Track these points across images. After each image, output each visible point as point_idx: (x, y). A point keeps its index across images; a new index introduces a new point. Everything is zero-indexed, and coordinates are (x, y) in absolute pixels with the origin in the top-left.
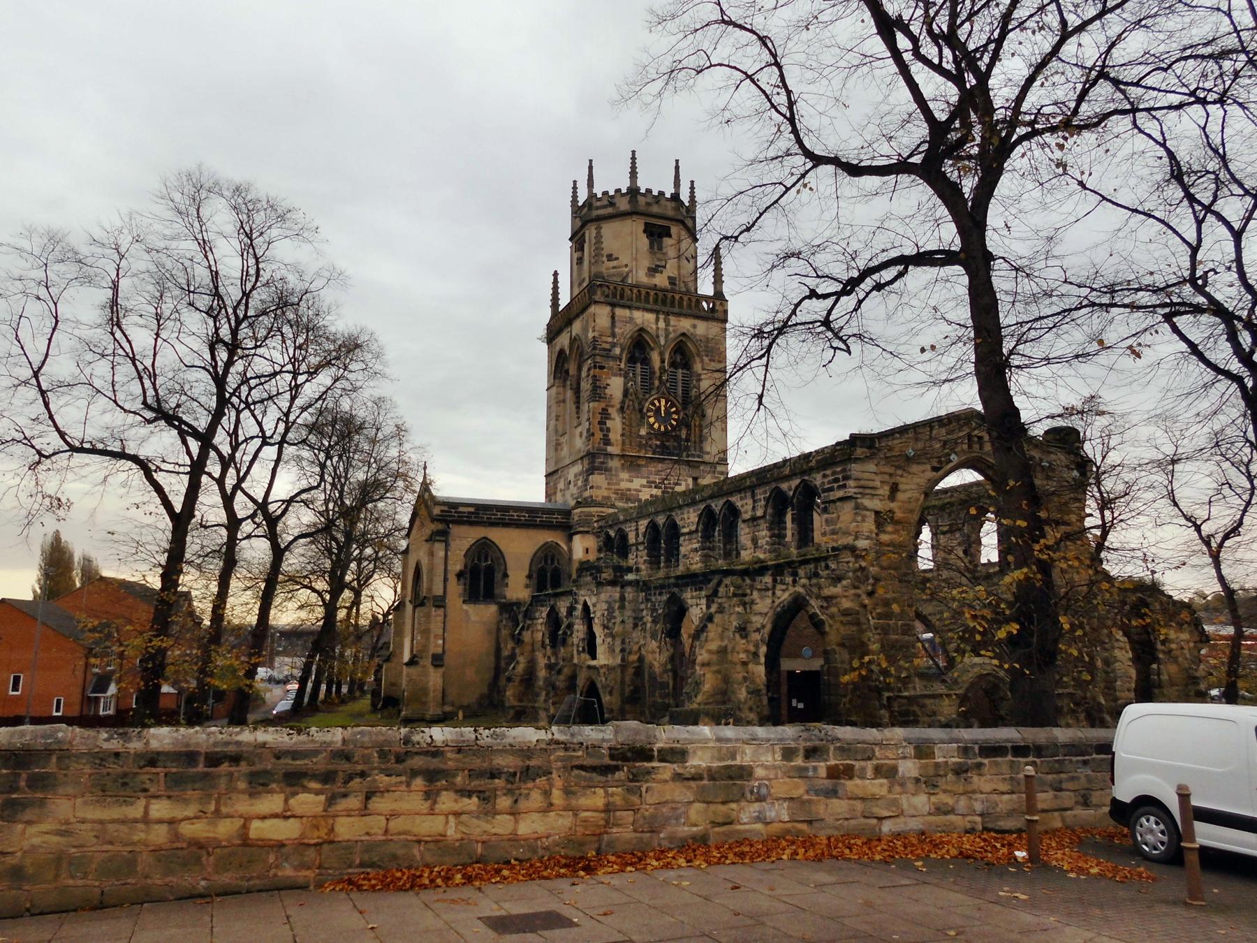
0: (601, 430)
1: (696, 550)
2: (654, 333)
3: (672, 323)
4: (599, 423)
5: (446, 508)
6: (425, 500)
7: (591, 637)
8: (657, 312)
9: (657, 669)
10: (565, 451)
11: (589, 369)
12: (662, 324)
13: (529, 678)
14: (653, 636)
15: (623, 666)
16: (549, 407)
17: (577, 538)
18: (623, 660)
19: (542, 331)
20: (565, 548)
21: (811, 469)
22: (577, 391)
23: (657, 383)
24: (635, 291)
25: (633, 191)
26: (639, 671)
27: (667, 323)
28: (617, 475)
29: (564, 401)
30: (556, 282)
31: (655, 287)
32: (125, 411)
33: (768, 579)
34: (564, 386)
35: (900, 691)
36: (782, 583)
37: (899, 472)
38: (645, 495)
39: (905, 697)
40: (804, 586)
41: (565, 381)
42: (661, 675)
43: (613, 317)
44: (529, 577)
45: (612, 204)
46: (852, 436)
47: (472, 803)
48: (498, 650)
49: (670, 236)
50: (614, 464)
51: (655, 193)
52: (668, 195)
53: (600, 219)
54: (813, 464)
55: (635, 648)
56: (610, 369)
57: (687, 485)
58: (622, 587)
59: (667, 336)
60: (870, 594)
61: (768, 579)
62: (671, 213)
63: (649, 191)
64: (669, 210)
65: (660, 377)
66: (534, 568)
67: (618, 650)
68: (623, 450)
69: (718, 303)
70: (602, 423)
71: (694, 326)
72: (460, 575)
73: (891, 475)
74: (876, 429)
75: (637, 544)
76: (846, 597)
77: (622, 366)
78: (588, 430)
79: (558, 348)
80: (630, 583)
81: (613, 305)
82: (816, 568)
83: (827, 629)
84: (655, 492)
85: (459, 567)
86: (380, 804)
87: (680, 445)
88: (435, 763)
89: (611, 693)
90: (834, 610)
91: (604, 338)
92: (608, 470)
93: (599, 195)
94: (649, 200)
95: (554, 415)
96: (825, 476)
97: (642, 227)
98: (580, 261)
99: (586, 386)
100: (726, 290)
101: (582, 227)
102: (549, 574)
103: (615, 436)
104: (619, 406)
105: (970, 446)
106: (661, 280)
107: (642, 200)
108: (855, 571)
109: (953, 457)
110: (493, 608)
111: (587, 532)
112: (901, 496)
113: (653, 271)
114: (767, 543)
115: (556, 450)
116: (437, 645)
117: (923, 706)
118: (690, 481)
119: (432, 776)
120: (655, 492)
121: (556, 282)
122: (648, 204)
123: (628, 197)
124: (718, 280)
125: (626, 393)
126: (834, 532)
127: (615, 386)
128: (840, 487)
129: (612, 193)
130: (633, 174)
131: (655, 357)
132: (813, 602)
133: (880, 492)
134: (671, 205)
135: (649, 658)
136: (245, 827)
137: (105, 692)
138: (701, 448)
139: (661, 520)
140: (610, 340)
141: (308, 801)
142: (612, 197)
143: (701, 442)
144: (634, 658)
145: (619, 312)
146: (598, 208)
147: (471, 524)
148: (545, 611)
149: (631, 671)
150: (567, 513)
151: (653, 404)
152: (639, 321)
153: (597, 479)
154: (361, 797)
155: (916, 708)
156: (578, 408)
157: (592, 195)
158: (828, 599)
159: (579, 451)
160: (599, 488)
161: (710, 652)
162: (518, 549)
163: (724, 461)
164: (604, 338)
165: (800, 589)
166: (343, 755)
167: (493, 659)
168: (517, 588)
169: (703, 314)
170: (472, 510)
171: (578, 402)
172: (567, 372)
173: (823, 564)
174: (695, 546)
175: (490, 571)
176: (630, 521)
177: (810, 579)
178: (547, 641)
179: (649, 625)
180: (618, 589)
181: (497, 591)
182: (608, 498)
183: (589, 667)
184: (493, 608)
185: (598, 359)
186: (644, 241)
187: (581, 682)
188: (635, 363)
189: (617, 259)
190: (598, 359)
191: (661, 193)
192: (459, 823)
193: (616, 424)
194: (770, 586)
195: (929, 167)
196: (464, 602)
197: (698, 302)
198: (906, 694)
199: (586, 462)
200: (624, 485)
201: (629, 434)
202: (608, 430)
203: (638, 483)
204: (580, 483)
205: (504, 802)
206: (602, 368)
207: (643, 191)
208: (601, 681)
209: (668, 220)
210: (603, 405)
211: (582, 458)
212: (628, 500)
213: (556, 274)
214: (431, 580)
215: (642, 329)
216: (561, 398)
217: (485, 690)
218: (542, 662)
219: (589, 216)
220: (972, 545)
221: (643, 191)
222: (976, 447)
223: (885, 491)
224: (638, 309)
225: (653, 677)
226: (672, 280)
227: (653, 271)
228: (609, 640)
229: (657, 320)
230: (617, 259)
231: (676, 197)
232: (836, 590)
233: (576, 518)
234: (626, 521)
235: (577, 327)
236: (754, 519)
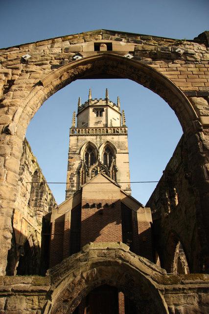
12: (98, 139)
27: (101, 139)
71: (113, 138)
73: (6, 74)
94: (96, 101)
113: (97, 123)
140: (76, 148)
229: (96, 139)
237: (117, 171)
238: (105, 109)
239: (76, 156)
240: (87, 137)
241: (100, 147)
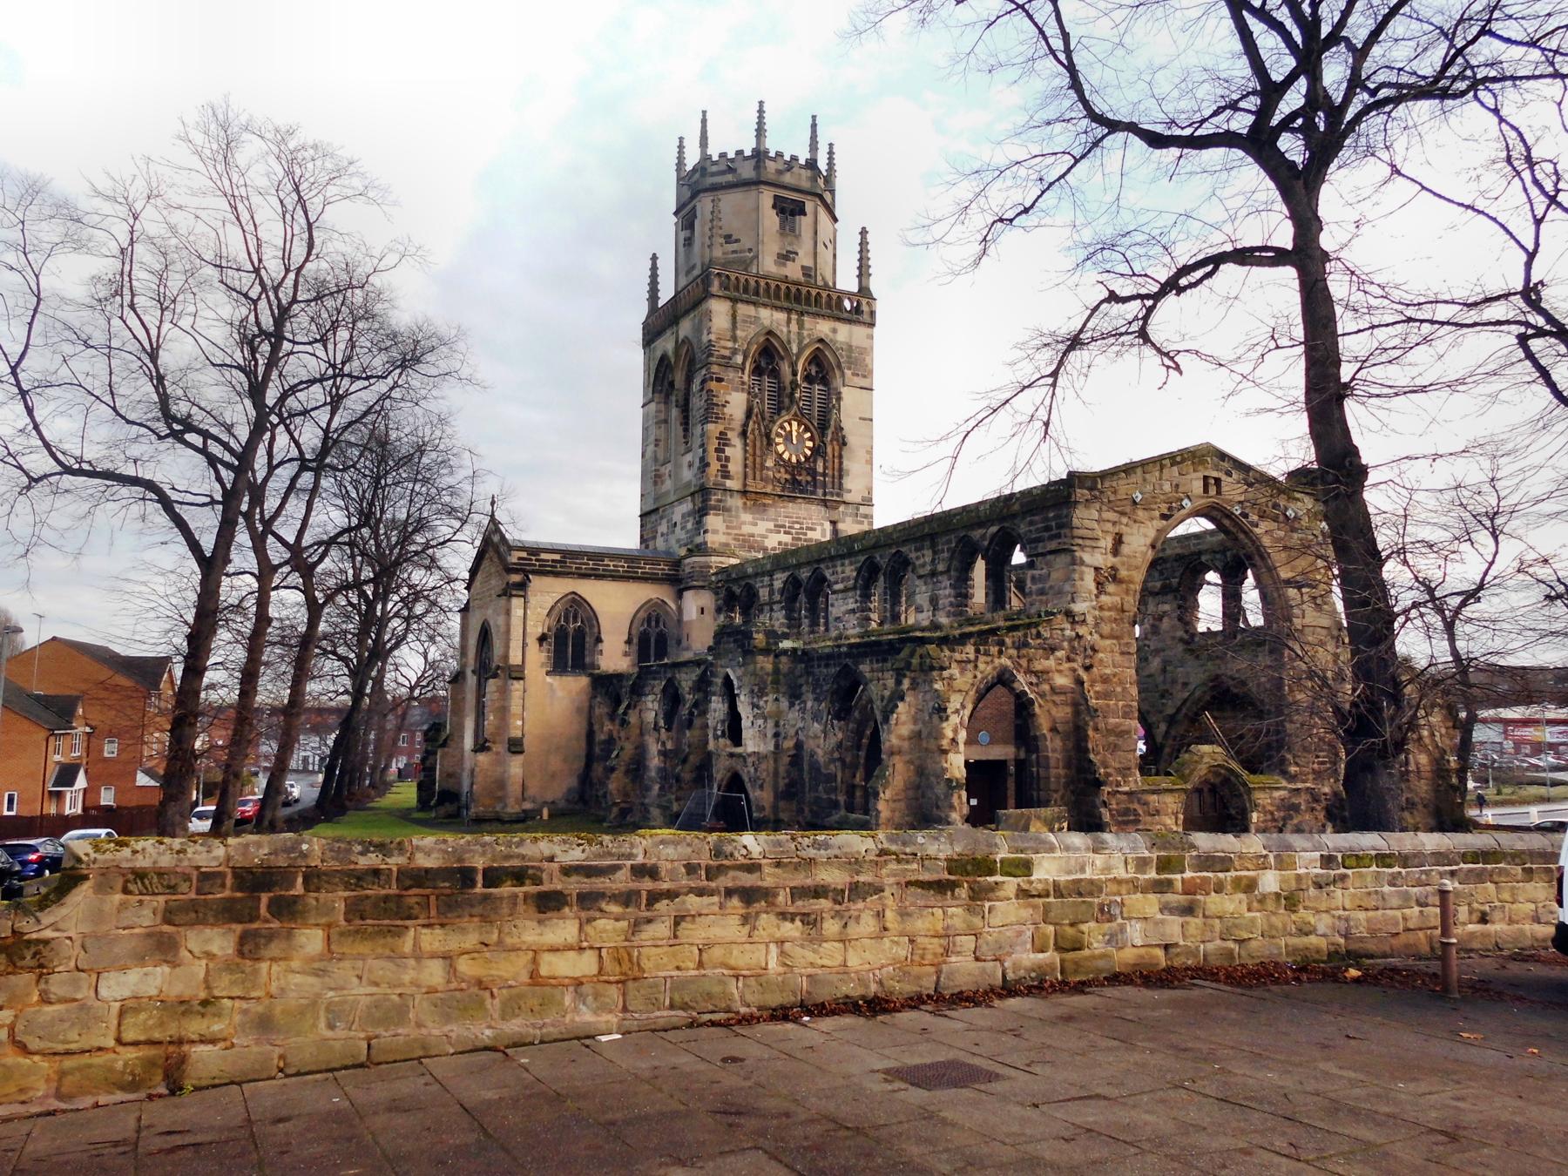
0: (719, 459)
1: (853, 611)
2: (784, 339)
3: (807, 325)
4: (717, 450)
5: (524, 555)
6: (493, 546)
7: (734, 720)
8: (789, 311)
9: (821, 755)
10: (668, 485)
11: (703, 382)
12: (794, 327)
13: (637, 767)
14: (816, 717)
16: (645, 429)
17: (688, 595)
18: (777, 746)
19: (638, 335)
20: (673, 606)
21: (1014, 516)
22: (685, 409)
23: (787, 400)
24: (762, 283)
25: (759, 155)
26: (796, 759)
27: (801, 325)
28: (737, 517)
29: (666, 421)
30: (654, 268)
31: (785, 280)
32: (128, 422)
33: (970, 649)
34: (666, 403)
35: (1119, 785)
36: (987, 654)
37: (1125, 520)
39: (1126, 793)
40: (1010, 658)
41: (667, 396)
42: (827, 767)
43: (734, 317)
44: (629, 642)
45: (731, 170)
46: (1071, 474)
47: (792, 929)
48: (590, 735)
50: (736, 502)
51: (787, 158)
52: (802, 161)
53: (715, 188)
54: (1016, 507)
55: (792, 732)
56: (730, 381)
57: (824, 531)
58: (776, 656)
59: (800, 342)
60: (1088, 668)
61: (970, 649)
62: (806, 185)
63: (779, 155)
64: (802, 179)
65: (792, 394)
66: (634, 632)
67: (770, 734)
68: (745, 485)
69: (864, 301)
71: (834, 331)
72: (542, 639)
73: (1114, 523)
74: (1098, 467)
75: (771, 603)
76: (1060, 671)
77: (746, 378)
78: (702, 459)
79: (659, 354)
80: (785, 652)
81: (734, 301)
82: (1025, 636)
83: (1037, 710)
84: (787, 539)
85: (539, 631)
86: (695, 933)
87: (814, 479)
88: (748, 880)
89: (761, 787)
90: (1046, 687)
91: (723, 343)
92: (727, 510)
93: (715, 158)
94: (781, 167)
95: (652, 438)
96: (1031, 523)
97: (771, 202)
98: (689, 242)
99: (697, 403)
100: (875, 286)
101: (693, 197)
102: (653, 637)
103: (735, 467)
104: (739, 429)
105: (1206, 490)
106: (793, 271)
107: (771, 166)
108: (1071, 640)
109: (1186, 502)
110: (583, 682)
111: (702, 587)
112: (1125, 549)
113: (786, 257)
114: (951, 604)
115: (655, 483)
116: (516, 728)
117: (1146, 804)
118: (828, 526)
119: (749, 896)
121: (654, 268)
122: (779, 172)
123: (753, 162)
124: (863, 270)
125: (749, 413)
126: (1042, 592)
127: (736, 403)
128: (1051, 538)
129: (731, 155)
130: (760, 131)
132: (1020, 677)
133: (1102, 543)
134: (806, 173)
135: (810, 744)
136: (535, 961)
137: (71, 784)
138: (841, 484)
139: (805, 574)
140: (730, 344)
141: (609, 927)
142: (732, 160)
143: (841, 477)
144: (788, 744)
145: (743, 309)
146: (713, 174)
147: (557, 574)
148: (659, 685)
149: (786, 760)
150: (677, 563)
151: (782, 427)
153: (713, 521)
154: (669, 922)
155: (1136, 806)
156: (686, 430)
157: (705, 158)
158: (1042, 675)
159: (688, 484)
160: (715, 532)
161: (901, 738)
162: (616, 606)
163: (868, 502)
164: (723, 343)
165: (1005, 661)
167: (583, 744)
168: (614, 656)
169: (846, 315)
170: (557, 557)
171: (685, 423)
172: (672, 384)
173: (1034, 631)
174: (851, 606)
175: (580, 635)
176: (763, 574)
177: (1018, 649)
178: (662, 723)
179: (809, 704)
180: (771, 658)
181: (587, 660)
182: (727, 545)
183: (732, 755)
184: (583, 682)
185: (715, 369)
186: (771, 219)
187: (720, 771)
188: (760, 375)
189: (737, 241)
190: (715, 369)
191: (794, 158)
192: (782, 953)
193: (735, 452)
194: (972, 657)
195: (1259, 143)
196: (548, 673)
197: (840, 301)
198: (1126, 789)
199: (698, 499)
200: (747, 529)
201: (753, 465)
202: (727, 459)
204: (689, 526)
205: (831, 927)
206: (720, 380)
207: (772, 154)
208: (747, 773)
209: (801, 192)
210: (721, 428)
211: (692, 494)
212: (751, 548)
213: (654, 258)
214: (507, 647)
215: (770, 333)
216: (662, 416)
217: (573, 782)
218: (653, 748)
219: (703, 185)
220: (1188, 607)
221: (772, 154)
222: (1213, 491)
223: (1108, 542)
224: (765, 305)
225: (815, 767)
226: (806, 271)
227: (786, 257)
228: (760, 722)
229: (789, 321)
230: (737, 241)
231: (812, 164)
232: (1050, 663)
233: (688, 570)
234: (756, 575)
235: (685, 328)
236: (933, 574)
237: (845, 444)
238: (809, 207)
239: (731, 375)
241: (798, 355)
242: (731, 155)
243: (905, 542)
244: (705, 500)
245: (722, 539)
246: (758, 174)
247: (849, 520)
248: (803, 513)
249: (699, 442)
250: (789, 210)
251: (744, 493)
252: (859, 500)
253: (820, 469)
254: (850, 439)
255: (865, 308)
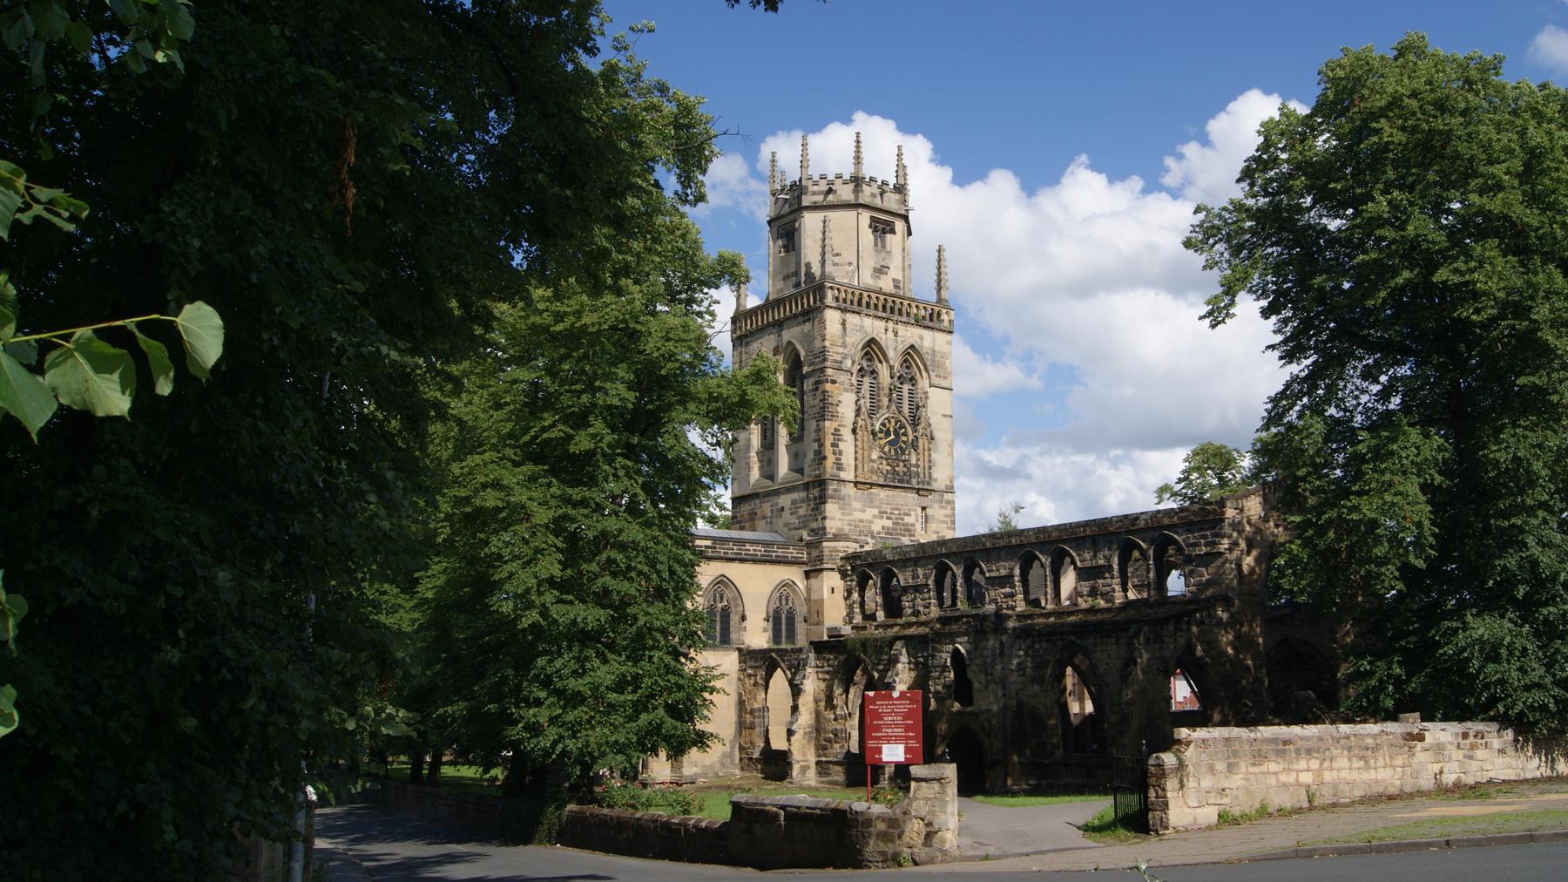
12: (890, 335)
15: (1004, 709)
23: (885, 401)
25: (857, 181)
31: (880, 292)
38: (877, 526)
43: (843, 324)
47: (1362, 763)
49: (893, 231)
50: (850, 490)
64: (891, 202)
70: (834, 445)
71: (921, 338)
84: (889, 523)
92: (841, 498)
93: (816, 178)
103: (848, 458)
106: (886, 284)
110: (735, 656)
113: (880, 271)
119: (1350, 749)
120: (889, 523)
123: (852, 186)
130: (858, 159)
131: (883, 371)
140: (841, 350)
141: (1314, 764)
144: (1014, 702)
145: (851, 318)
146: (814, 193)
152: (869, 330)
153: (831, 508)
160: (833, 518)
163: (950, 490)
164: (835, 349)
166: (1320, 739)
170: (709, 543)
175: (726, 614)
181: (733, 636)
186: (867, 236)
200: (858, 515)
202: (841, 453)
203: (870, 513)
206: (834, 382)
210: (835, 425)
227: (880, 271)
238: (899, 225)
239: (842, 378)
240: (868, 322)
242: (831, 177)
243: (1064, 541)
244: (824, 490)
245: (839, 524)
246: (857, 197)
247: (936, 505)
248: (901, 501)
249: (813, 436)
250: (882, 228)
251: (856, 484)
252: (943, 488)
253: (914, 461)
254: (937, 434)
255: (944, 317)
